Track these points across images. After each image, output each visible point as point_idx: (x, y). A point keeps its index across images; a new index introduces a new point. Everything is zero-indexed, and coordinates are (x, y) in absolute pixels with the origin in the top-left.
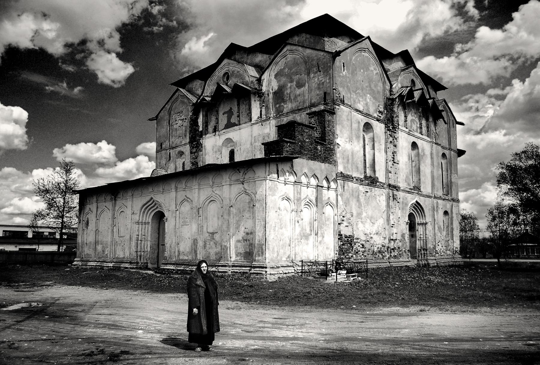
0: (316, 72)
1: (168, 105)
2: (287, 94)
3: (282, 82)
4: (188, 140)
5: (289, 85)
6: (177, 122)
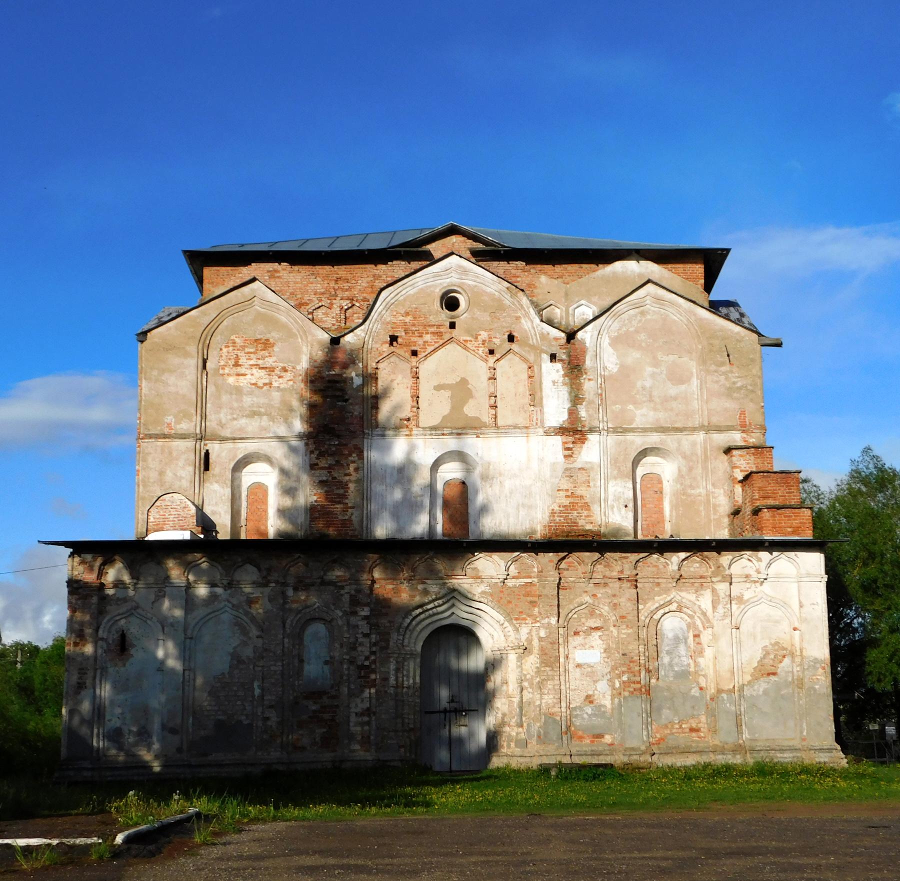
0: (722, 364)
1: (205, 314)
2: (644, 388)
3: (629, 360)
5: (649, 369)
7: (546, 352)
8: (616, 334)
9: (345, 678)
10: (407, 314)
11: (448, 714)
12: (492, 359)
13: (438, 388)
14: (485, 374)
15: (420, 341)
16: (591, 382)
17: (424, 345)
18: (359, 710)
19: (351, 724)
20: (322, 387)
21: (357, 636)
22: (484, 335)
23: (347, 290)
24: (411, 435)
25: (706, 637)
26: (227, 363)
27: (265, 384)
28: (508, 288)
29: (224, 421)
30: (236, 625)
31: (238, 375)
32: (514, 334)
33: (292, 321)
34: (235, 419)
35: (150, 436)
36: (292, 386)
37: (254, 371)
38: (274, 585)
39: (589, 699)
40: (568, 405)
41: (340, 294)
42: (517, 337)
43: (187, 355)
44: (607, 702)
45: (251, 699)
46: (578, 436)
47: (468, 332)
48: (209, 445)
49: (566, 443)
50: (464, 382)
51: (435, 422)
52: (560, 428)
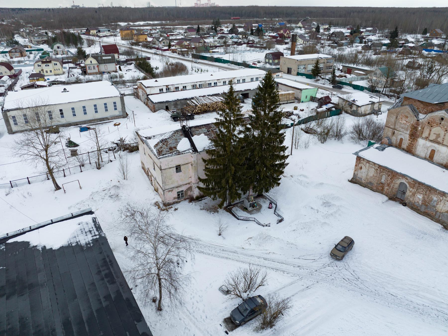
4: (408, 132)
10: (432, 119)
12: (446, 132)
13: (434, 134)
14: (443, 134)
22: (446, 127)
25: (439, 203)
39: (418, 202)
43: (394, 115)
44: (420, 204)
47: (443, 126)
50: (439, 134)
51: (432, 139)
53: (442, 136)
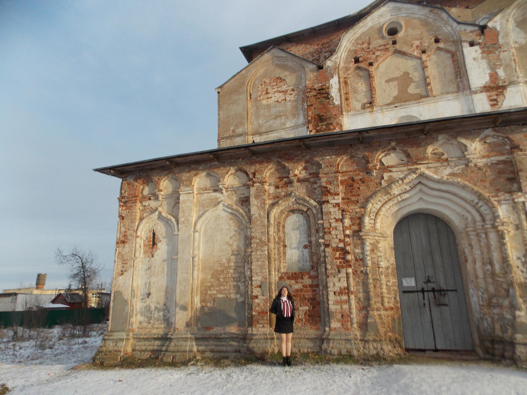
6: (270, 95)
7: (466, 41)
8: (521, 19)
9: (322, 259)
11: (426, 294)
13: (388, 81)
15: (374, 56)
16: (506, 53)
17: (377, 58)
18: (337, 289)
19: (331, 302)
20: (315, 94)
21: (330, 221)
22: (417, 43)
23: (328, 47)
24: (373, 111)
26: (262, 93)
27: (282, 100)
28: (431, 11)
29: (261, 124)
30: (231, 220)
31: (268, 98)
32: (440, 37)
33: (295, 63)
34: (266, 122)
35: (224, 138)
36: (298, 98)
37: (276, 94)
38: (258, 184)
40: (488, 71)
41: (324, 50)
42: (441, 39)
45: (243, 280)
46: (500, 90)
48: (254, 138)
49: (491, 96)
50: (406, 74)
52: (485, 87)
53: (416, 76)
